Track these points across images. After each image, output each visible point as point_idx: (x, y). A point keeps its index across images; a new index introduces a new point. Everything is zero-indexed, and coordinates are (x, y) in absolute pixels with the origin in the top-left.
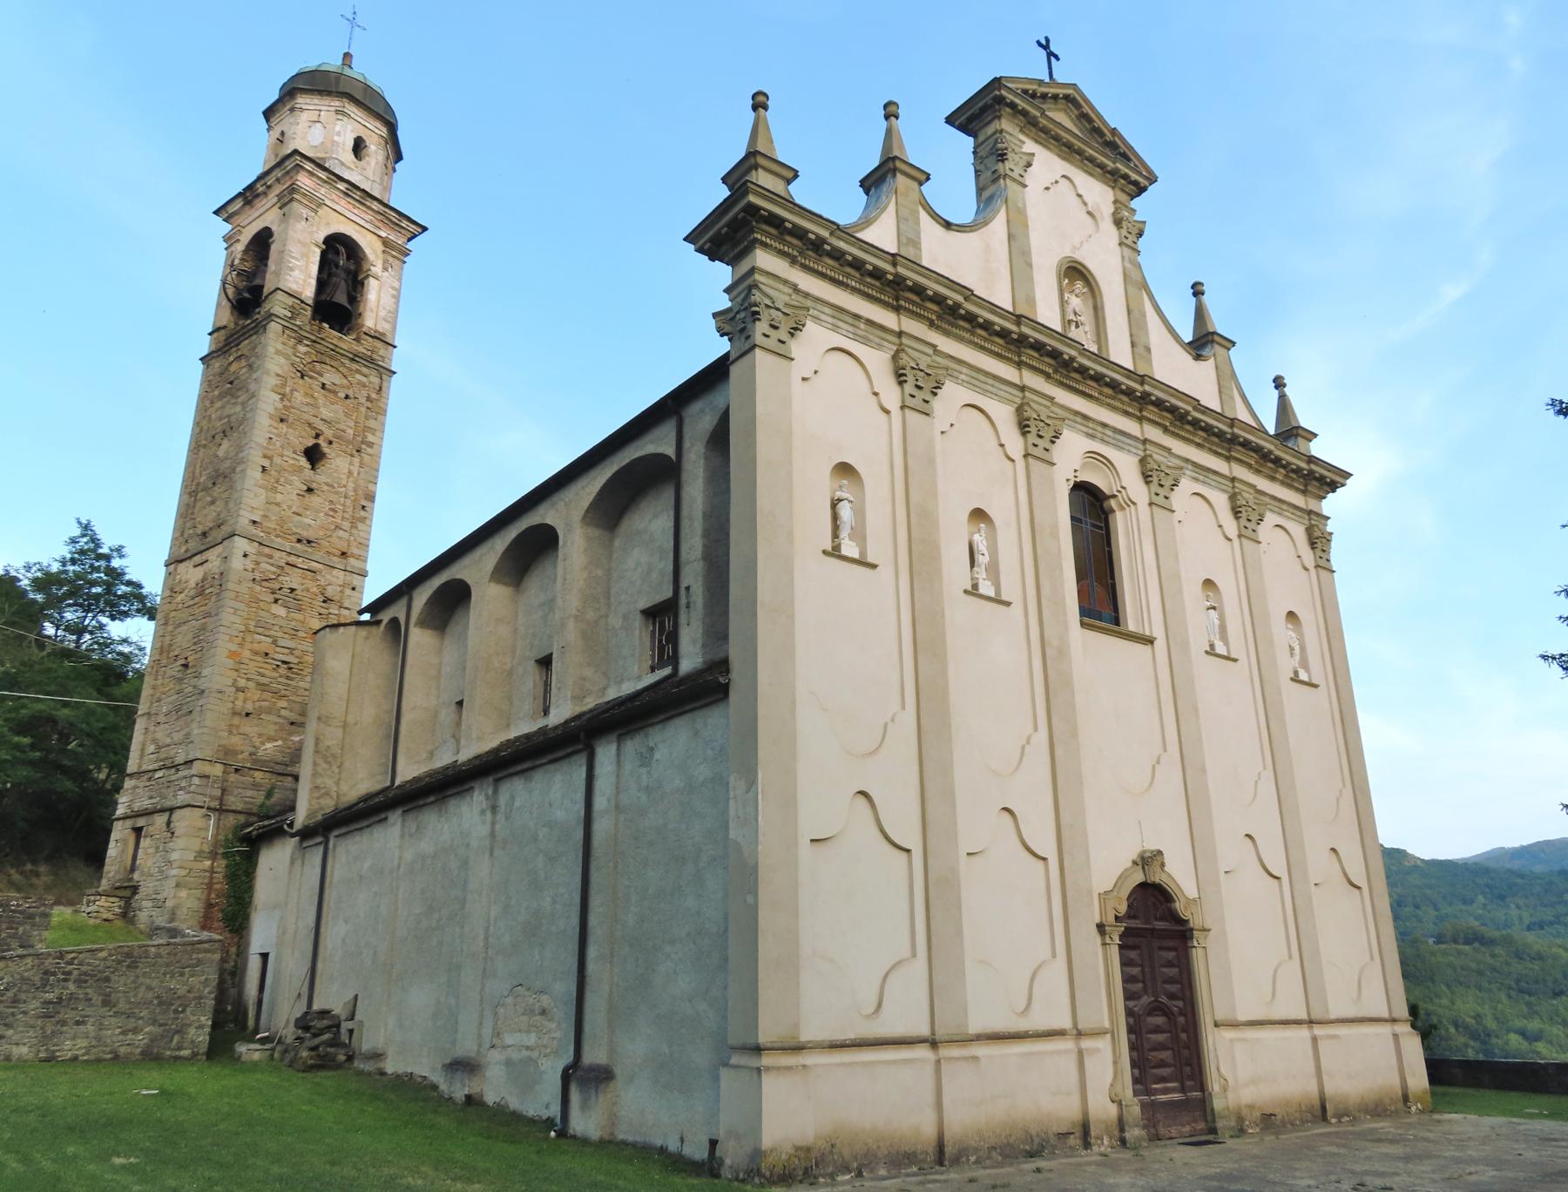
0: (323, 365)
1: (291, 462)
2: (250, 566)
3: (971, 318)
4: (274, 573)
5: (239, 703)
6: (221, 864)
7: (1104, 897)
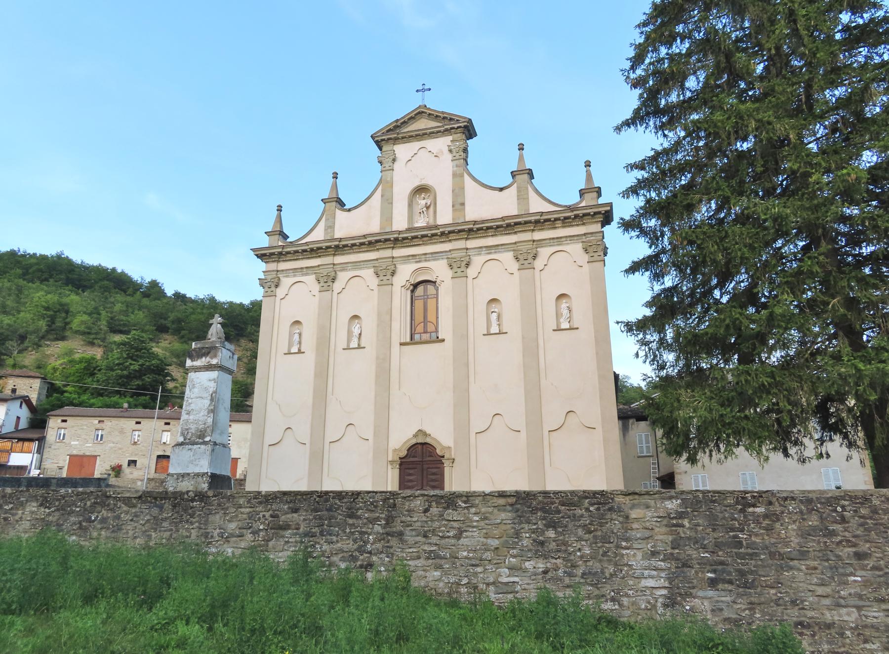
3: (346, 246)
7: (395, 450)
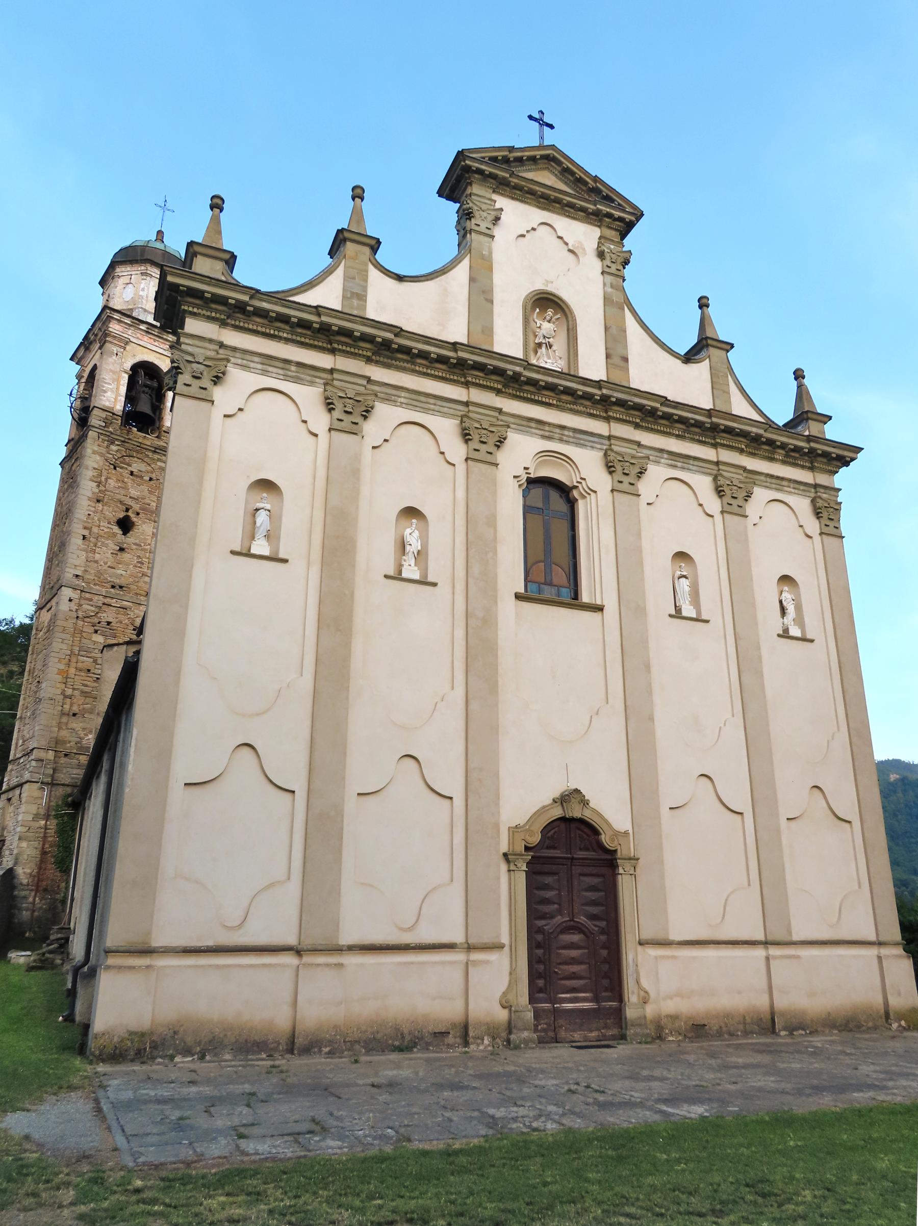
0: (131, 458)
1: (106, 530)
2: (74, 608)
3: (407, 351)
4: (93, 611)
5: (67, 707)
6: (53, 824)
7: (514, 830)
